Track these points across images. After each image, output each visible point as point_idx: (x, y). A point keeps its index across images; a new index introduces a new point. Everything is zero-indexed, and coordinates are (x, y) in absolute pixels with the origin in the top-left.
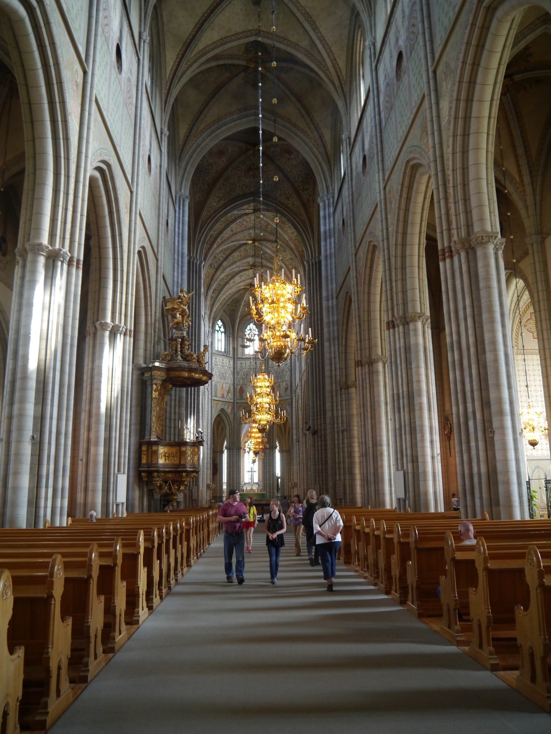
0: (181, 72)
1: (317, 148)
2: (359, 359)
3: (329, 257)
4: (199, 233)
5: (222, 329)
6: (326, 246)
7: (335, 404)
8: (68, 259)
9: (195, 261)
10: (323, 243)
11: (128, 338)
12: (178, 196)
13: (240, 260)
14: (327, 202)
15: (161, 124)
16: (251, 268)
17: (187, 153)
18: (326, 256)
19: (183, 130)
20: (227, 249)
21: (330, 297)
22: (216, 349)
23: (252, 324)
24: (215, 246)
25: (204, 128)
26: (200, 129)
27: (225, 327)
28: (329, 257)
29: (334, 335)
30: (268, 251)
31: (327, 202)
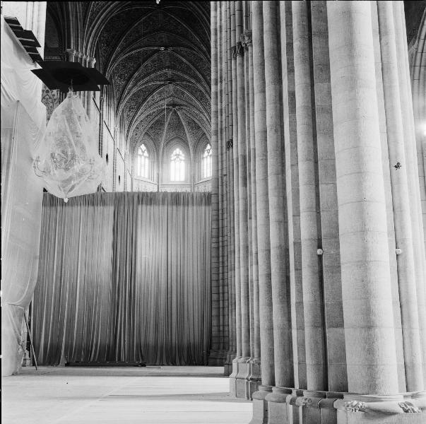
2: (230, 138)
3: (218, 29)
4: (91, 23)
5: (146, 154)
6: (216, 17)
7: (220, 212)
9: (84, 57)
10: (212, 13)
13: (154, 72)
16: (169, 83)
18: (216, 30)
21: (219, 80)
22: (139, 175)
27: (149, 152)
28: (218, 29)
29: (221, 125)
30: (184, 60)
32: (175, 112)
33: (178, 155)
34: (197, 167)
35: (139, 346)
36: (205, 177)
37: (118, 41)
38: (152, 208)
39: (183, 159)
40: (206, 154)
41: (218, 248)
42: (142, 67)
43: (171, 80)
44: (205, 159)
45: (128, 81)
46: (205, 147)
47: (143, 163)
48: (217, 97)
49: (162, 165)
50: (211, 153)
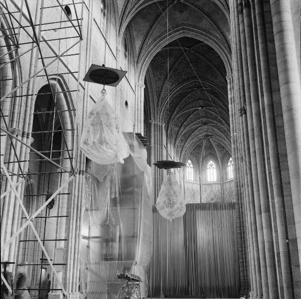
0: (127, 12)
1: (223, 45)
4: (161, 106)
5: (192, 166)
6: (232, 108)
8: (21, 133)
10: (230, 106)
11: (81, 175)
12: (136, 85)
14: (231, 79)
15: (117, 44)
17: (142, 58)
18: (232, 114)
19: (138, 44)
20: (186, 113)
23: (211, 161)
24: (175, 112)
25: (152, 42)
26: (149, 43)
27: (194, 165)
31: (231, 79)
32: (208, 139)
33: (211, 165)
34: (224, 172)
35: (202, 288)
36: (230, 178)
37: (175, 109)
38: (202, 212)
39: (215, 167)
40: (229, 164)
41: (241, 233)
42: (188, 119)
43: (205, 124)
44: (229, 167)
45: (180, 128)
46: (229, 158)
47: (190, 172)
48: (235, 151)
49: (202, 171)
50: (232, 163)
